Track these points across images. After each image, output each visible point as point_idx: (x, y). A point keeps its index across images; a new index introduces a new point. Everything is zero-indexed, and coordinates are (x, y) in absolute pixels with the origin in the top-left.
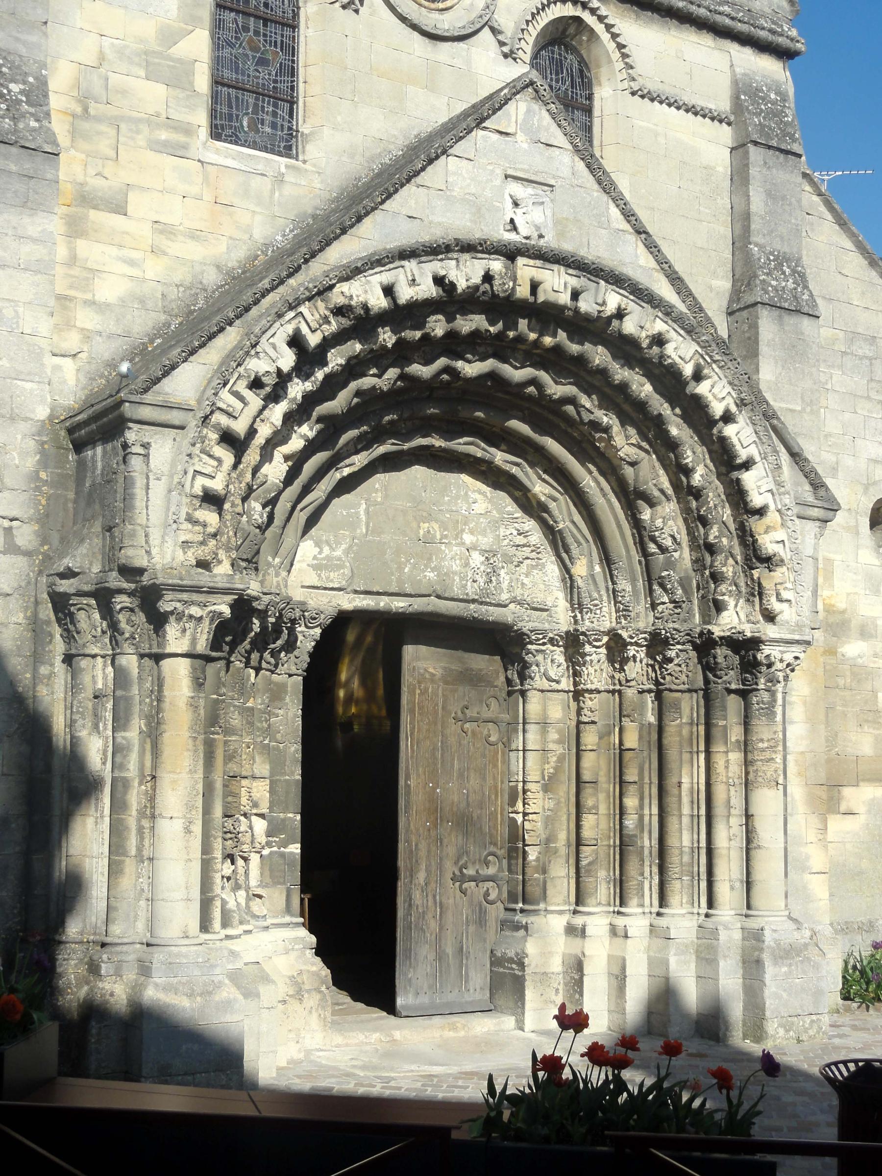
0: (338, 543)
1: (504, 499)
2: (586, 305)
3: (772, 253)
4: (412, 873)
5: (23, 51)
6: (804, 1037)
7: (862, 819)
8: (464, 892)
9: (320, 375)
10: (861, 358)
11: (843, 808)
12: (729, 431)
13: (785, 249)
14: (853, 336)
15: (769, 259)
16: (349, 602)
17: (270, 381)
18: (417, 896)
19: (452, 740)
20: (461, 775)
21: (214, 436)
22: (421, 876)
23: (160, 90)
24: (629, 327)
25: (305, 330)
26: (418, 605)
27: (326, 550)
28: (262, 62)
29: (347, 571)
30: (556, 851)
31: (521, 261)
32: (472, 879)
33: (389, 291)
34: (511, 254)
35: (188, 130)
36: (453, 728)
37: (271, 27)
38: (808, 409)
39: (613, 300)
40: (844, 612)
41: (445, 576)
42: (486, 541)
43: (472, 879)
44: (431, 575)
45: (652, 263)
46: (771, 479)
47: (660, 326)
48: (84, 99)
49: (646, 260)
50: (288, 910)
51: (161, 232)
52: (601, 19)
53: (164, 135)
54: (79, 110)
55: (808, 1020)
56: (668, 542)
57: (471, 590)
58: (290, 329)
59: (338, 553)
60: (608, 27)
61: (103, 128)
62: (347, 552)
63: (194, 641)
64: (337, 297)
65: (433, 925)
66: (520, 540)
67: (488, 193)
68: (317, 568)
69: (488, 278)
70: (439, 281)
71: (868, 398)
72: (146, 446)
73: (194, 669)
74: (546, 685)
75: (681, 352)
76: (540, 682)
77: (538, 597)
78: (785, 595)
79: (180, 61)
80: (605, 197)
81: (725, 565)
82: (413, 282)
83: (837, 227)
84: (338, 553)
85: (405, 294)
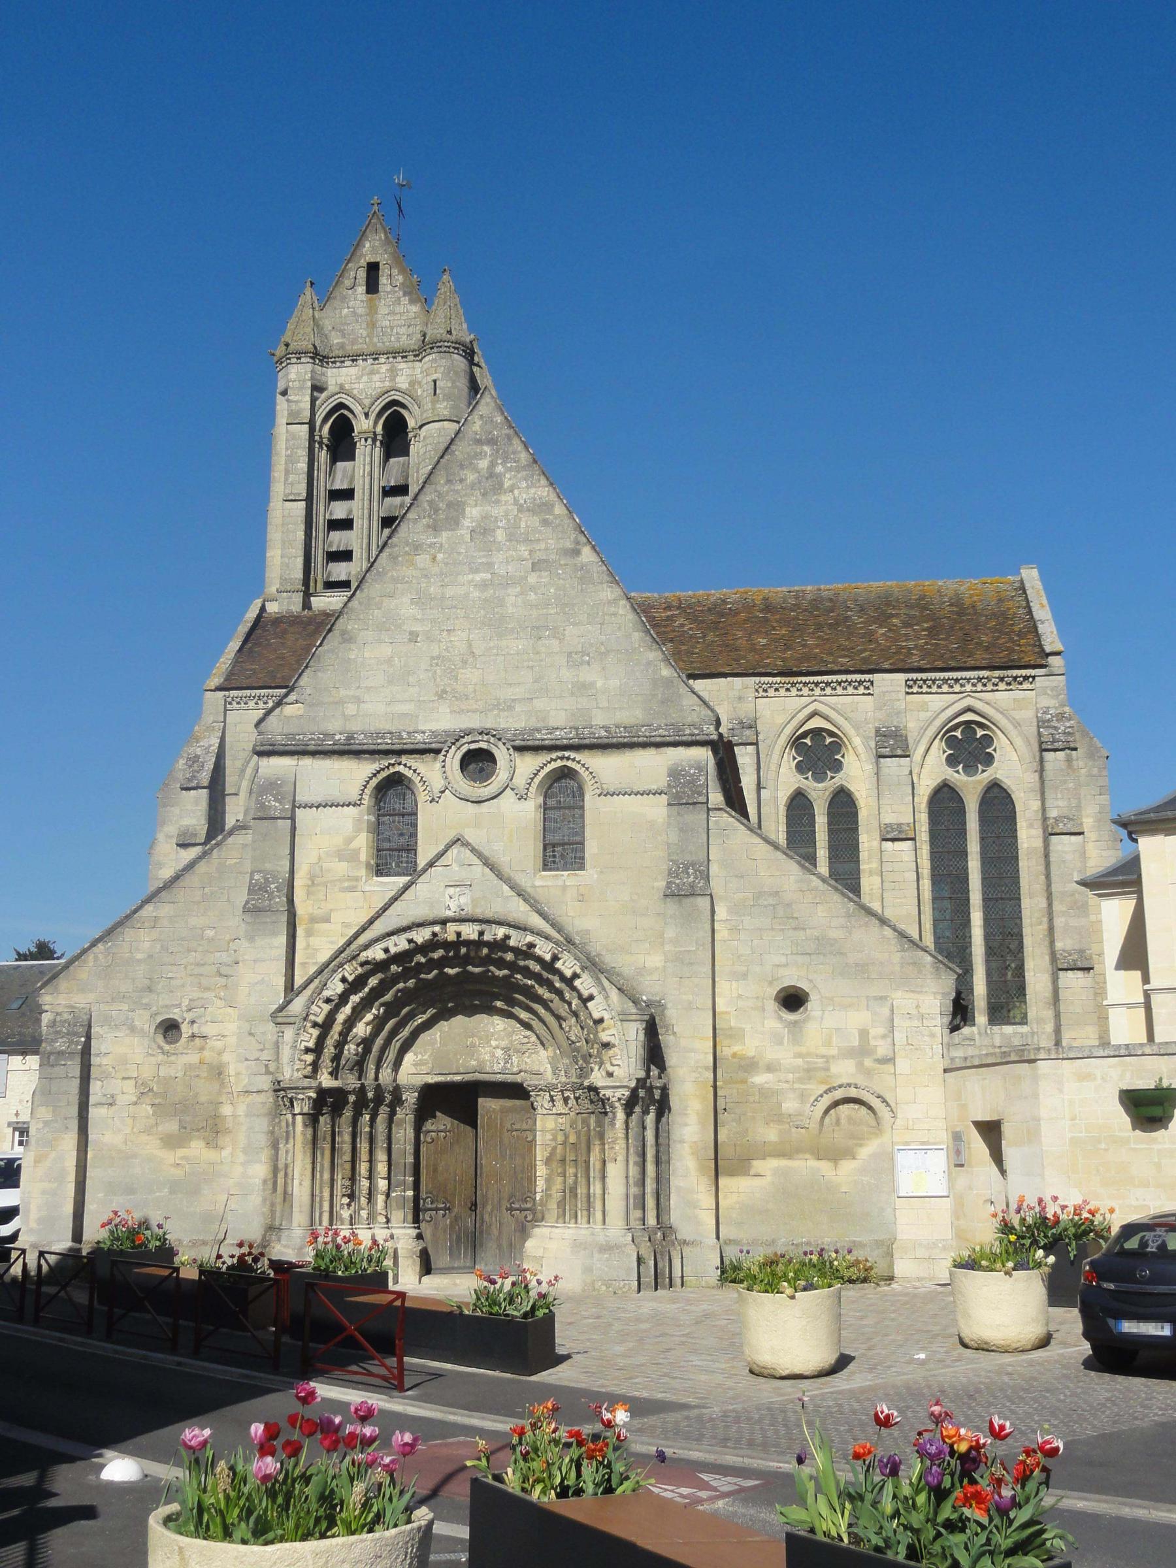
0: (425, 1052)
1: (513, 1022)
2: (487, 937)
3: (682, 863)
4: (484, 1207)
5: (279, 869)
6: (620, 1292)
7: (769, 1179)
8: (513, 1216)
9: (367, 990)
10: (765, 906)
12: (577, 983)
13: (694, 858)
14: (759, 895)
15: (679, 868)
16: (431, 1079)
17: (336, 998)
18: (486, 1217)
19: (506, 1141)
20: (511, 1157)
21: (309, 1025)
22: (489, 1208)
23: (344, 865)
24: (512, 943)
25: (347, 975)
26: (467, 1078)
27: (420, 1057)
28: (402, 835)
29: (430, 1065)
30: (550, 1195)
31: (448, 925)
33: (386, 950)
34: (444, 922)
35: (357, 879)
36: (506, 1134)
37: (406, 817)
38: (701, 948)
40: (754, 1057)
41: (482, 1063)
42: (503, 1044)
44: (473, 1063)
45: (528, 908)
46: (605, 1003)
47: (530, 938)
48: (312, 878)
49: (523, 907)
51: (346, 926)
52: (579, 762)
53: (346, 884)
54: (310, 883)
55: (622, 1283)
56: (573, 1038)
57: (497, 1068)
58: (340, 976)
59: (425, 1057)
60: (583, 765)
61: (319, 888)
62: (430, 1056)
63: (302, 1109)
64: (364, 956)
65: (495, 1232)
66: (526, 1040)
67: (437, 896)
68: (415, 1065)
69: (434, 935)
70: (410, 941)
71: (773, 929)
72: (283, 1032)
73: (303, 1119)
74: (545, 1112)
75: (544, 950)
76: (539, 1111)
77: (535, 1068)
78: (615, 1062)
79: (354, 850)
80: (501, 882)
81: (592, 1048)
82: (396, 945)
83: (749, 832)
84: (425, 1057)
85: (393, 950)
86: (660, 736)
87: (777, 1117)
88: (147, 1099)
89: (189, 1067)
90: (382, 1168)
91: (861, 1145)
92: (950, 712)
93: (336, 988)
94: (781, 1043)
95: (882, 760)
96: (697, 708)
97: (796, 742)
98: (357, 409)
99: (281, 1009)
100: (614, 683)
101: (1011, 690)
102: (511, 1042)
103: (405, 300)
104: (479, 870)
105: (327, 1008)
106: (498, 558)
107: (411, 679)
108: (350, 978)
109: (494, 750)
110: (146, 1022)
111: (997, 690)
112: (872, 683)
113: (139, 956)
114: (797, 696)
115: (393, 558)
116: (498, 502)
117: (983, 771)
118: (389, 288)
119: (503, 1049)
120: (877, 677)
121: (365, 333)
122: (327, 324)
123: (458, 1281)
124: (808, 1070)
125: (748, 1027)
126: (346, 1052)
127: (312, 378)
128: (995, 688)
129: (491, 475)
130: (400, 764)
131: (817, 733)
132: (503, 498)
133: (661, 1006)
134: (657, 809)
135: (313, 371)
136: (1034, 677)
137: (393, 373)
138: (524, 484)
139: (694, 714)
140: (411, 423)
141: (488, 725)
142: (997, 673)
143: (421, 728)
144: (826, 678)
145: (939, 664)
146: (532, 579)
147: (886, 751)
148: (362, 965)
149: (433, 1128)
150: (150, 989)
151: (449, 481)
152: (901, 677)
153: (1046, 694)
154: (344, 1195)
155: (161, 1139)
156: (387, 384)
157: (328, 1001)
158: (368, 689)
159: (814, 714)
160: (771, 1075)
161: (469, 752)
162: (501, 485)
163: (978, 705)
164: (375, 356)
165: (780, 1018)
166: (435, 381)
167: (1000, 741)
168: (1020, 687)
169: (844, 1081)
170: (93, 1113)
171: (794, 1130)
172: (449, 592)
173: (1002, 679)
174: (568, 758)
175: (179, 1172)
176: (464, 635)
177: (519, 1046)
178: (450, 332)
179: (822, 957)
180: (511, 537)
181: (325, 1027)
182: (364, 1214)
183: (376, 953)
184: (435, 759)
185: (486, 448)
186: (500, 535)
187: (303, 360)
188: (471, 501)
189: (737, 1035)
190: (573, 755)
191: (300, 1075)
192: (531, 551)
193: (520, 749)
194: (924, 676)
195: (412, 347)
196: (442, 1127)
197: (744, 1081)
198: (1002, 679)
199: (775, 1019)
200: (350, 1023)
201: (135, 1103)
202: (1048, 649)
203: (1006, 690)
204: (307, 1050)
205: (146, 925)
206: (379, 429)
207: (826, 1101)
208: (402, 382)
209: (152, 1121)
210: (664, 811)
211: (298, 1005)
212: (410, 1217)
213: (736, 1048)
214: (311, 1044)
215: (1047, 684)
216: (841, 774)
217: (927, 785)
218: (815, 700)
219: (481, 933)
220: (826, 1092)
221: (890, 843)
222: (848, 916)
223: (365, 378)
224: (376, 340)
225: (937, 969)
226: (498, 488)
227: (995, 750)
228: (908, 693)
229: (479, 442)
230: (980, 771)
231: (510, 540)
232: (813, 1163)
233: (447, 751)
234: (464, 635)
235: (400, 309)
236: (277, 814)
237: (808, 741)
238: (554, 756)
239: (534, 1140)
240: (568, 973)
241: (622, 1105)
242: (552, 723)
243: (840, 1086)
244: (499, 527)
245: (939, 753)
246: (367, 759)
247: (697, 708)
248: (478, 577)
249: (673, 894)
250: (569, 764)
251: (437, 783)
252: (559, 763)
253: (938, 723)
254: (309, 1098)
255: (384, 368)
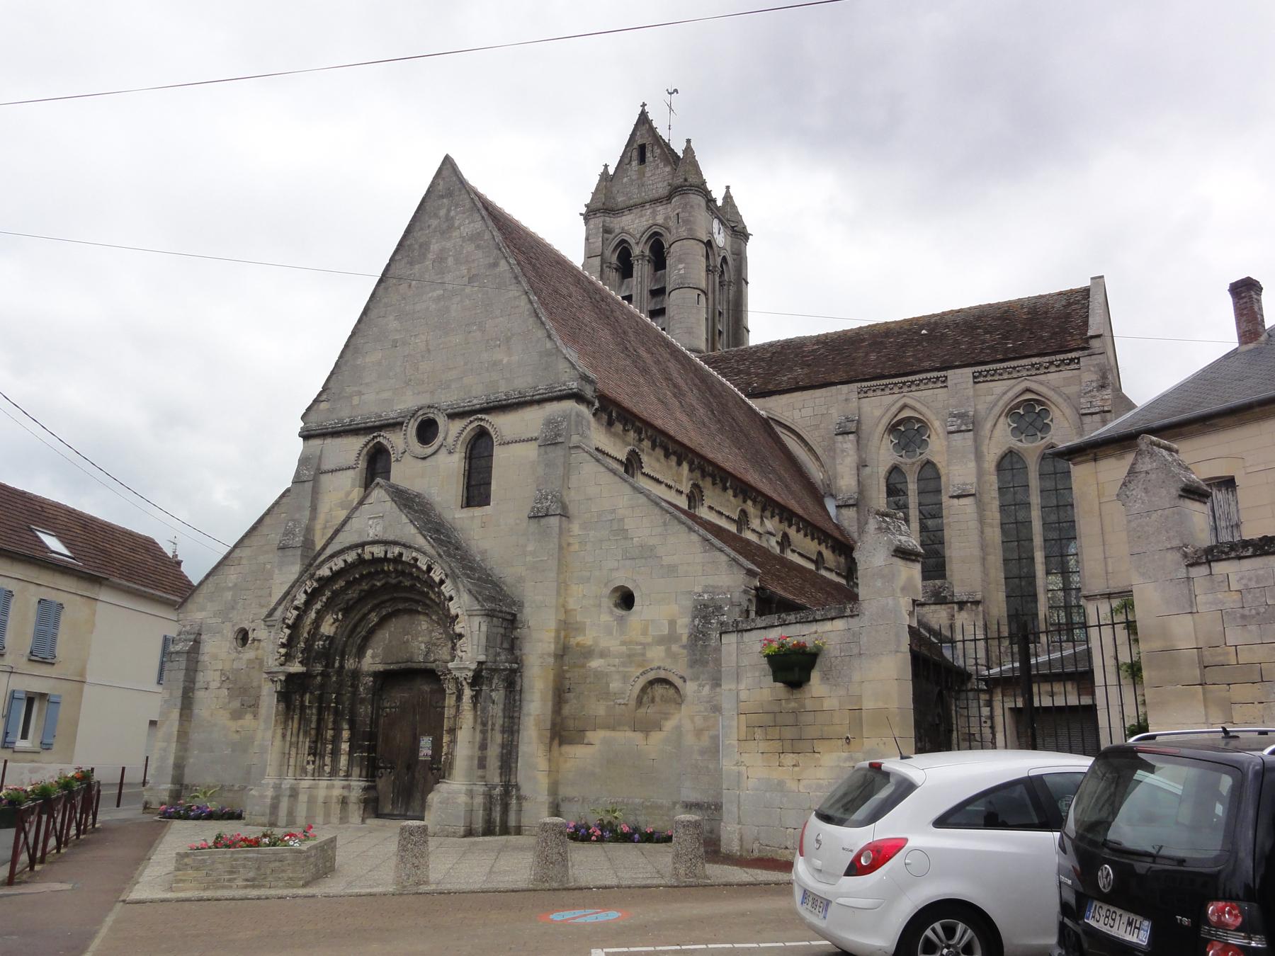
10: (606, 521)
11: (586, 741)
18: (417, 775)
26: (403, 666)
32: (435, 769)
34: (363, 545)
39: (397, 550)
40: (591, 646)
42: (426, 639)
43: (435, 769)
47: (414, 554)
50: (360, 776)
69: (359, 555)
70: (345, 561)
76: (448, 691)
78: (464, 649)
86: (539, 394)
87: (606, 694)
88: (226, 685)
89: (250, 661)
90: (346, 734)
91: (666, 719)
92: (1011, 394)
93: (301, 599)
94: (610, 633)
95: (951, 436)
96: (568, 370)
97: (893, 429)
98: (632, 241)
99: (270, 614)
100: (515, 358)
101: (1061, 371)
102: (431, 638)
103: (661, 165)
104: (389, 506)
105: (295, 613)
106: (448, 277)
107: (391, 374)
108: (309, 591)
109: (437, 419)
110: (229, 632)
111: (1049, 372)
112: (946, 377)
113: (230, 585)
114: (890, 394)
115: (386, 289)
116: (450, 237)
117: (1042, 438)
118: (651, 159)
119: (425, 643)
120: (950, 373)
121: (637, 191)
122: (615, 190)
123: (387, 824)
124: (629, 656)
125: (588, 621)
126: (316, 647)
127: (603, 226)
128: (1046, 371)
129: (448, 219)
130: (380, 436)
131: (908, 419)
132: (454, 234)
133: (521, 605)
134: (530, 451)
135: (604, 222)
136: (1078, 359)
137: (654, 213)
138: (467, 221)
139: (566, 375)
140: (666, 246)
141: (435, 401)
142: (1047, 359)
143: (395, 408)
144: (911, 378)
145: (1000, 357)
146: (468, 290)
147: (952, 428)
148: (320, 579)
149: (388, 705)
150: (233, 608)
151: (422, 229)
152: (968, 371)
153: (1090, 370)
154: (309, 755)
155: (230, 713)
156: (651, 222)
157: (297, 608)
158: (367, 384)
159: (905, 406)
160: (602, 660)
161: (422, 421)
162: (453, 225)
163: (1034, 386)
164: (642, 205)
165: (611, 612)
166: (678, 214)
167: (1055, 412)
168: (1068, 367)
169: (656, 664)
170: (200, 695)
171: (617, 706)
172: (418, 307)
173: (1051, 363)
174: (481, 420)
175: (236, 737)
176: (423, 337)
177: (435, 641)
178: (686, 180)
179: (643, 560)
180: (457, 262)
181: (295, 627)
182: (327, 769)
183: (325, 572)
184: (401, 429)
185: (445, 200)
186: (450, 261)
187: (598, 215)
188: (434, 241)
189: (580, 629)
190: (483, 416)
191: (277, 663)
192: (469, 270)
193: (452, 416)
194: (987, 367)
195: (666, 195)
196: (394, 705)
197: (583, 666)
198: (1051, 363)
199: (607, 615)
200: (317, 623)
201: (219, 688)
202: (1090, 333)
203: (1057, 371)
204: (283, 645)
205: (236, 562)
206: (647, 252)
207: (642, 682)
208: (660, 220)
209: (227, 700)
210: (536, 452)
211: (278, 614)
212: (364, 773)
213: (579, 639)
214: (284, 641)
215: (1090, 362)
216: (927, 451)
217: (992, 453)
218: (904, 396)
219: (386, 552)
220: (641, 674)
221: (956, 501)
222: (665, 524)
223: (637, 221)
224: (643, 194)
225: (731, 565)
226: (451, 228)
227: (1051, 420)
228: (975, 383)
229: (442, 197)
230: (1039, 438)
231: (456, 264)
232: (630, 734)
233: (408, 423)
234: (423, 337)
235: (659, 171)
236: (305, 479)
237: (902, 428)
238: (472, 419)
239: (443, 714)
240: (437, 579)
241: (468, 683)
242: (474, 394)
243: (652, 669)
244: (450, 256)
245: (1004, 426)
246: (362, 434)
247: (568, 370)
248: (435, 294)
249: (536, 517)
250: (482, 424)
251: (401, 448)
252: (476, 424)
253: (1001, 403)
254: (281, 680)
255: (649, 211)
